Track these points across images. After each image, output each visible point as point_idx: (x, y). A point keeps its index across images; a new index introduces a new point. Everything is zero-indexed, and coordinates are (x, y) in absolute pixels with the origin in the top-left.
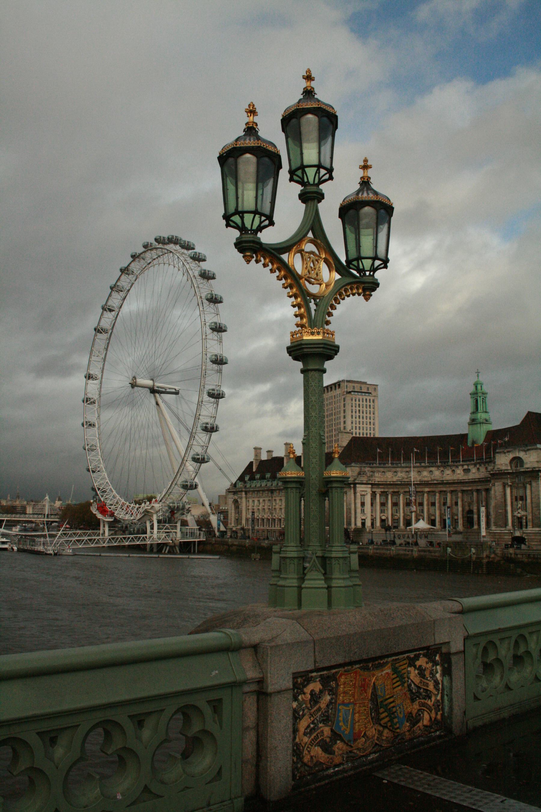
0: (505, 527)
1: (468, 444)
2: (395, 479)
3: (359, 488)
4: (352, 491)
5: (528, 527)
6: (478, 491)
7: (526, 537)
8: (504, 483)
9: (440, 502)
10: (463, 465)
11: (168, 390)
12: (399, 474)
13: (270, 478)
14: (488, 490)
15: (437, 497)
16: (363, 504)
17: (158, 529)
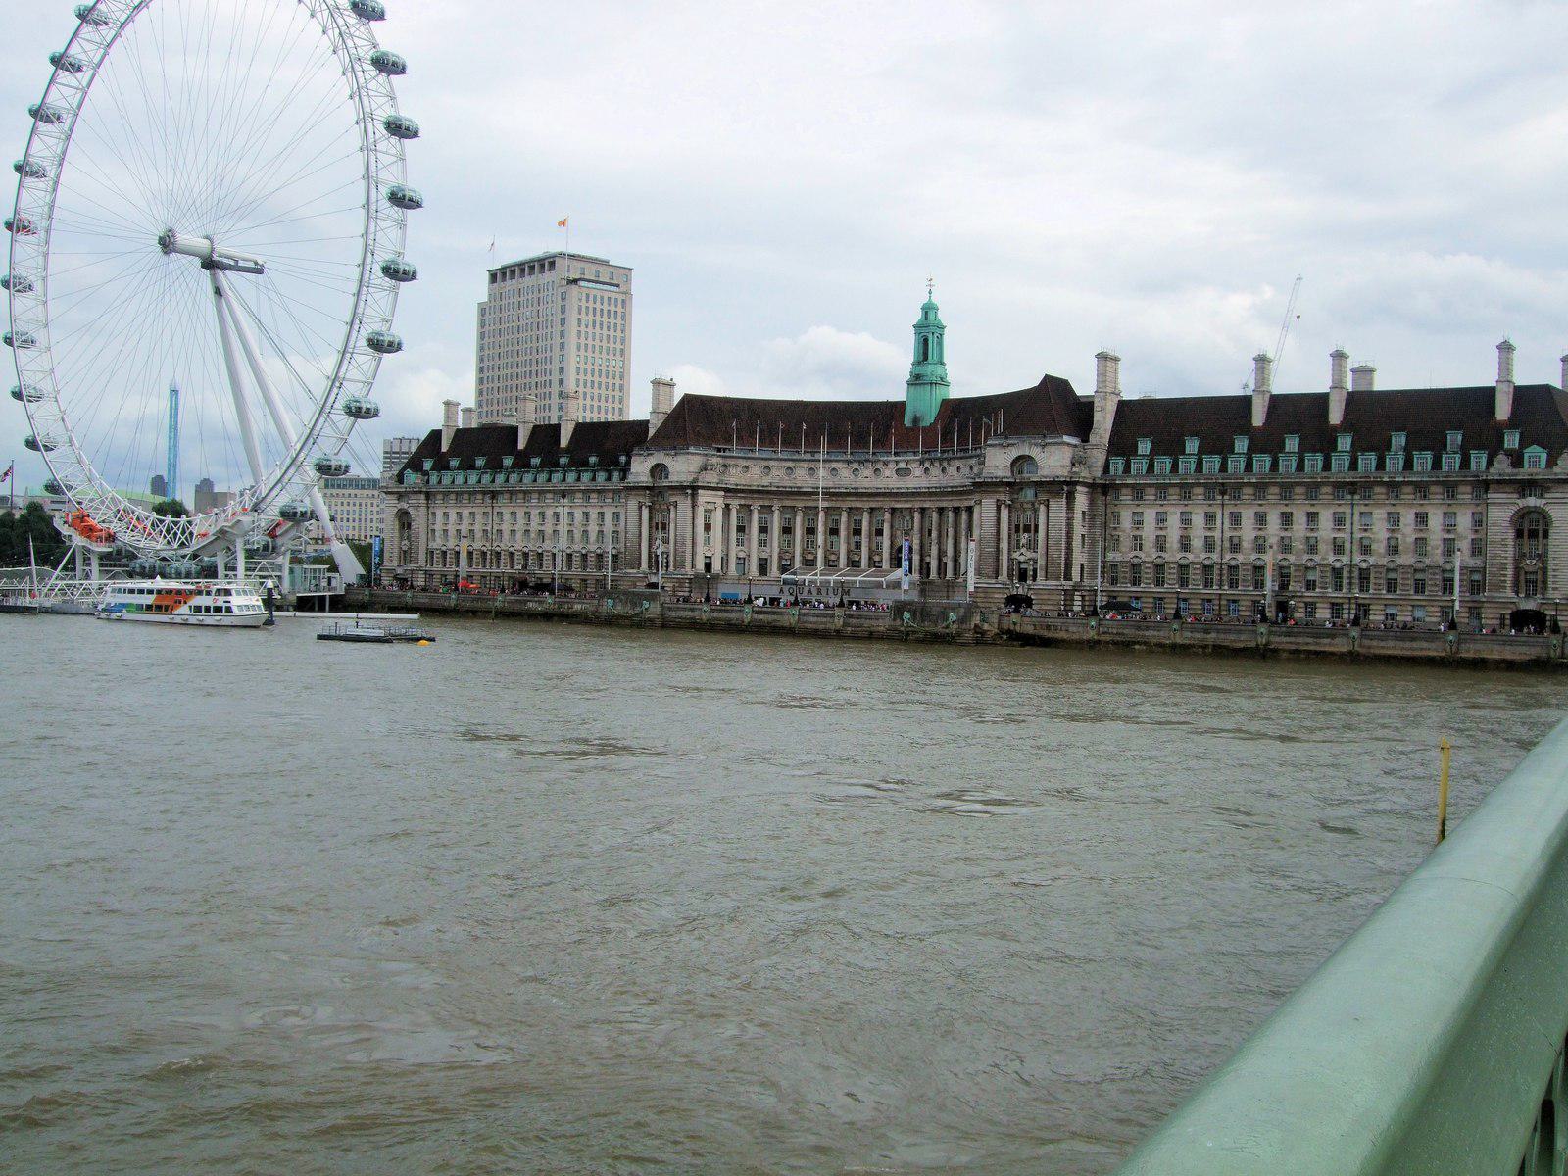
2: (766, 481)
3: (703, 497)
4: (689, 501)
5: (1038, 578)
7: (1032, 597)
9: (848, 528)
12: (774, 472)
15: (844, 519)
16: (708, 528)
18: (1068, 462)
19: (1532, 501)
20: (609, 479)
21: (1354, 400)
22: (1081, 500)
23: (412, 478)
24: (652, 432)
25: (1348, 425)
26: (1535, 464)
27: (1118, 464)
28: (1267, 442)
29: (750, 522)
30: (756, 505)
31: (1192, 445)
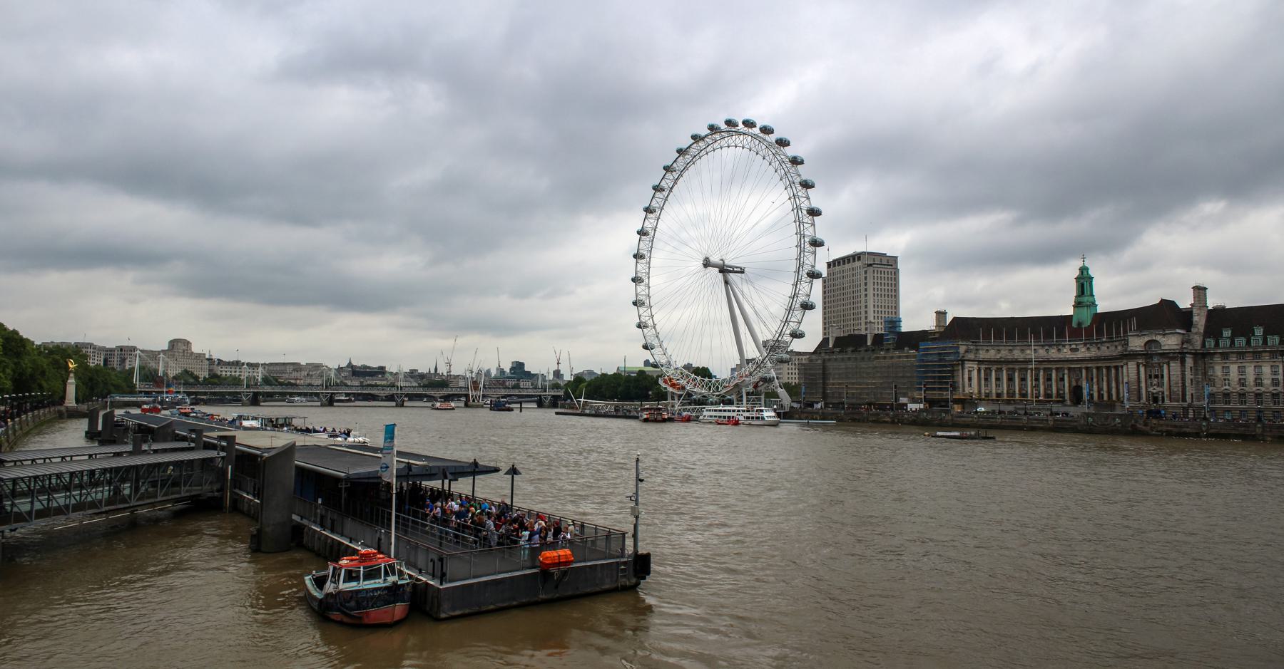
0: (1139, 401)
1: (1073, 325)
3: (968, 365)
6: (1087, 368)
8: (1138, 363)
9: (1044, 378)
11: (735, 269)
12: (1002, 352)
14: (1116, 368)
16: (970, 379)
17: (747, 401)
18: (1180, 342)
22: (1189, 362)
27: (1210, 343)
29: (991, 375)
30: (994, 368)
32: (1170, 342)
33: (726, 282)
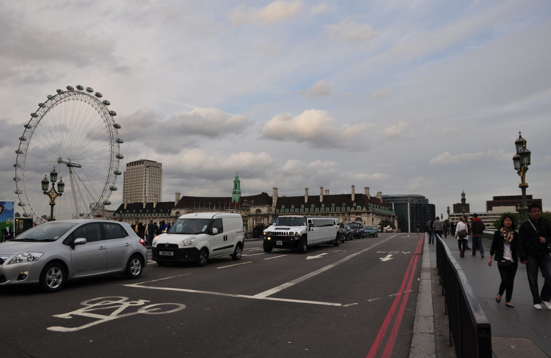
10: (230, 210)
11: (76, 165)
13: (136, 212)
18: (268, 210)
19: (359, 216)
20: (165, 215)
21: (325, 197)
23: (117, 215)
24: (175, 204)
25: (323, 202)
26: (359, 209)
27: (278, 211)
28: (308, 206)
31: (293, 207)
32: (264, 210)
33: (71, 172)
